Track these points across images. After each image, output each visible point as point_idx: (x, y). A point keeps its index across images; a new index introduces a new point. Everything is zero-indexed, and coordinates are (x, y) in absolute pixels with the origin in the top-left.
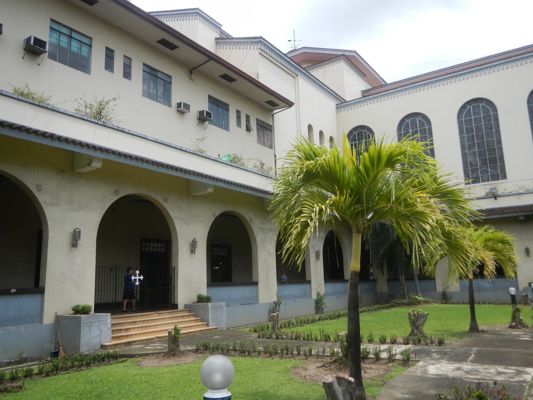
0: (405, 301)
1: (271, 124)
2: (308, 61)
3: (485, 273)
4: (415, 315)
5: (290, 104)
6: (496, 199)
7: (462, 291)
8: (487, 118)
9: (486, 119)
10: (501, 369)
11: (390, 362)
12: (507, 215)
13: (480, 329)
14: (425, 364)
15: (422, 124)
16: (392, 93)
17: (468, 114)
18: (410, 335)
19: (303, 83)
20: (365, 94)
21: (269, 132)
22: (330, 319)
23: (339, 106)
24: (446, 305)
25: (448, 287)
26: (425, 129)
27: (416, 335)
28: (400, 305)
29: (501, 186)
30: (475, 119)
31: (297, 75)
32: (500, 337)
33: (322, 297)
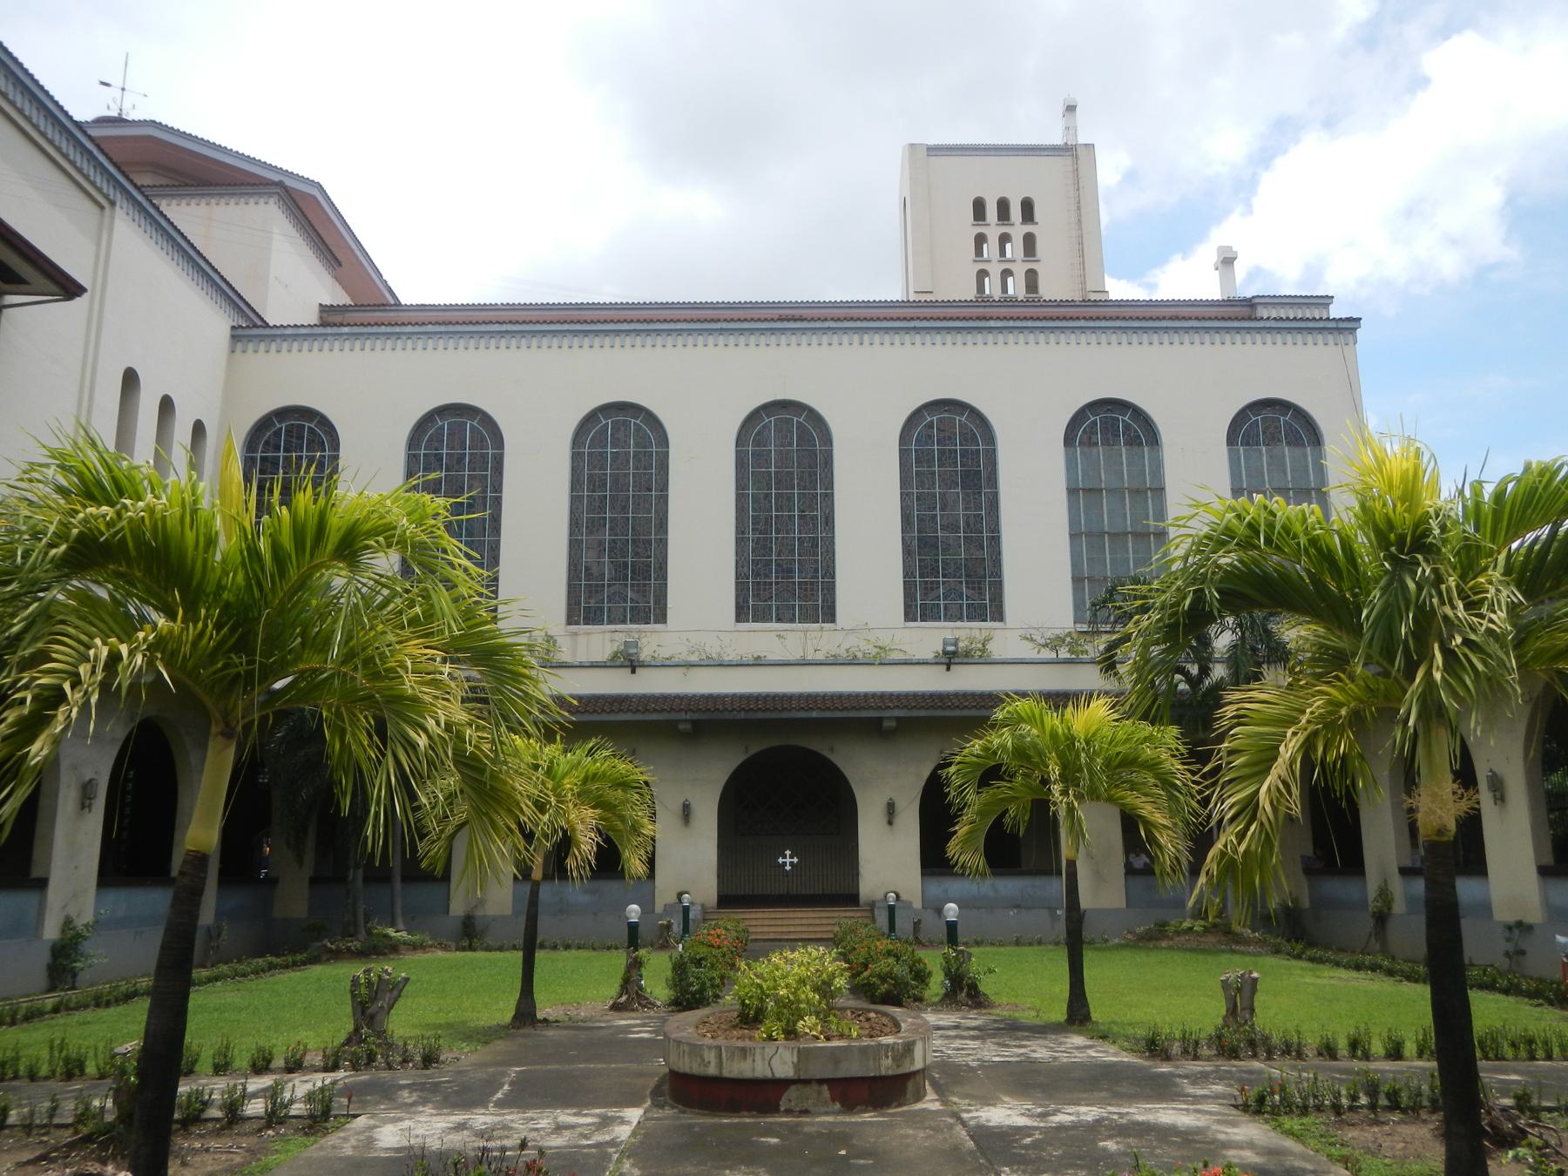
0: (355, 945)
2: (157, 167)
3: (570, 863)
4: (369, 983)
5: (69, 289)
6: (633, 672)
7: (516, 914)
8: (643, 459)
9: (639, 461)
10: (566, 1117)
11: (269, 1126)
12: (654, 717)
13: (540, 1016)
14: (372, 1122)
15: (479, 441)
16: (410, 335)
17: (600, 440)
18: (348, 1041)
19: (127, 232)
20: (330, 317)
22: (98, 1005)
23: (240, 332)
24: (469, 954)
25: (482, 902)
26: (484, 456)
27: (364, 1041)
28: (336, 956)
29: (652, 640)
30: (615, 456)
31: (113, 204)
32: (583, 1035)
33: (79, 935)
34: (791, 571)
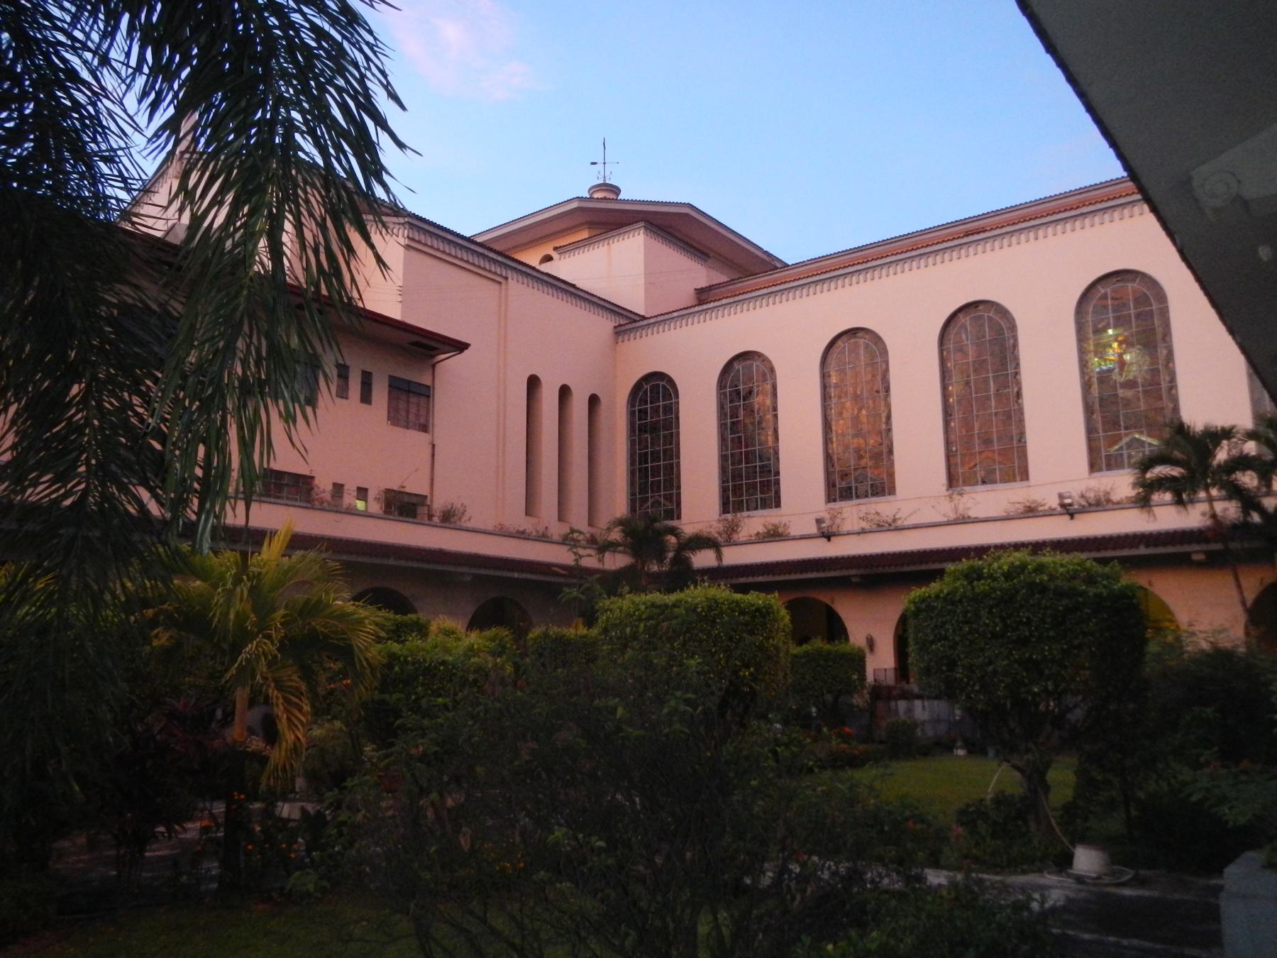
1: (428, 383)
5: (461, 347)
20: (704, 296)
21: (423, 400)
34: (992, 442)
